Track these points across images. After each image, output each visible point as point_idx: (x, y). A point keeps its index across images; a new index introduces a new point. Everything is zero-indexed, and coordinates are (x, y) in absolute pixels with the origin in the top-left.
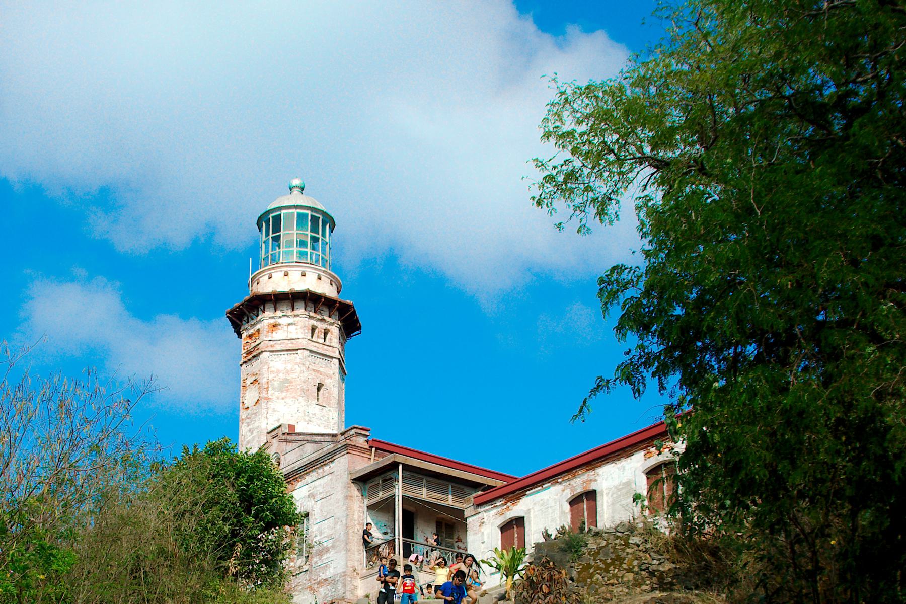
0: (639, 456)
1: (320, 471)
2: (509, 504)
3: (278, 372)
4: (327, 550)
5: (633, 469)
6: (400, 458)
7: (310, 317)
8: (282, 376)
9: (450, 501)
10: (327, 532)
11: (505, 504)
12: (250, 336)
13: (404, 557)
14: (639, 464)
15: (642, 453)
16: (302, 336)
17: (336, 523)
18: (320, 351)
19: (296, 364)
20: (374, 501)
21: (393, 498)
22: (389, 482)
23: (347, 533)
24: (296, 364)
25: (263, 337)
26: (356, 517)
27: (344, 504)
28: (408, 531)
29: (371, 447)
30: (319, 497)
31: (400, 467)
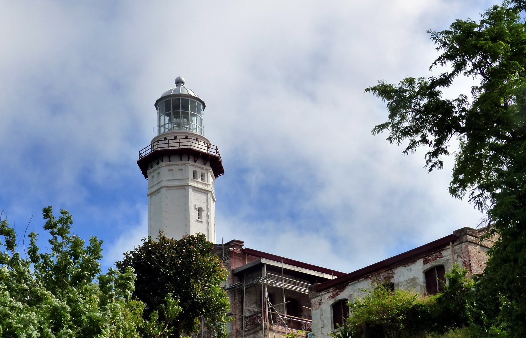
0: (420, 262)
2: (338, 291)
5: (417, 271)
6: (264, 261)
11: (335, 290)
14: (420, 268)
15: (422, 260)
29: (245, 253)
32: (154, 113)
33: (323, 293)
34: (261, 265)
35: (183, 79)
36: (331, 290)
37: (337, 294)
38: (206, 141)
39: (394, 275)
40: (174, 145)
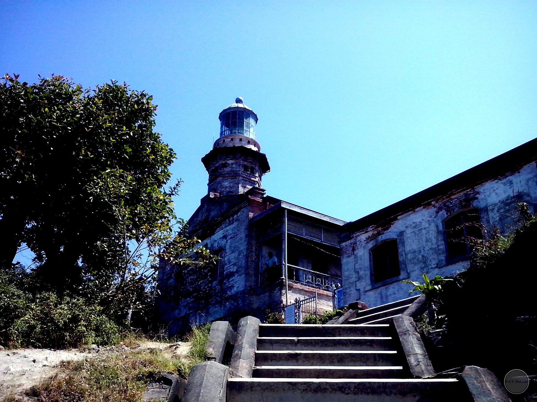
2: (380, 229)
3: (226, 187)
4: (232, 274)
8: (228, 189)
16: (238, 169)
17: (239, 254)
19: (236, 183)
23: (247, 262)
24: (236, 183)
27: (245, 241)
30: (229, 237)
31: (286, 210)
32: (218, 123)
33: (358, 234)
35: (240, 98)
36: (369, 229)
37: (379, 234)
38: (256, 144)
39: (477, 196)
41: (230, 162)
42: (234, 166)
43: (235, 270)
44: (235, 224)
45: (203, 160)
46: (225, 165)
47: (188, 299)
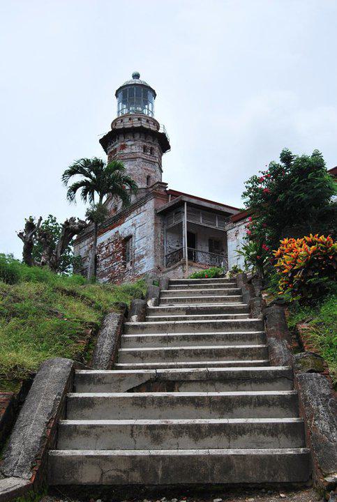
1: (139, 209)
4: (142, 257)
6: (186, 199)
7: (143, 141)
9: (217, 226)
10: (142, 246)
12: (111, 153)
13: (188, 259)
16: (138, 151)
18: (148, 159)
20: (171, 226)
21: (181, 224)
22: (180, 213)
25: (118, 152)
26: (159, 236)
28: (192, 242)
32: (115, 101)
34: (181, 203)
36: (247, 220)
40: (128, 125)
41: (129, 143)
42: (133, 147)
43: (144, 253)
44: (143, 214)
45: (102, 141)
46: (123, 147)
47: (104, 279)
